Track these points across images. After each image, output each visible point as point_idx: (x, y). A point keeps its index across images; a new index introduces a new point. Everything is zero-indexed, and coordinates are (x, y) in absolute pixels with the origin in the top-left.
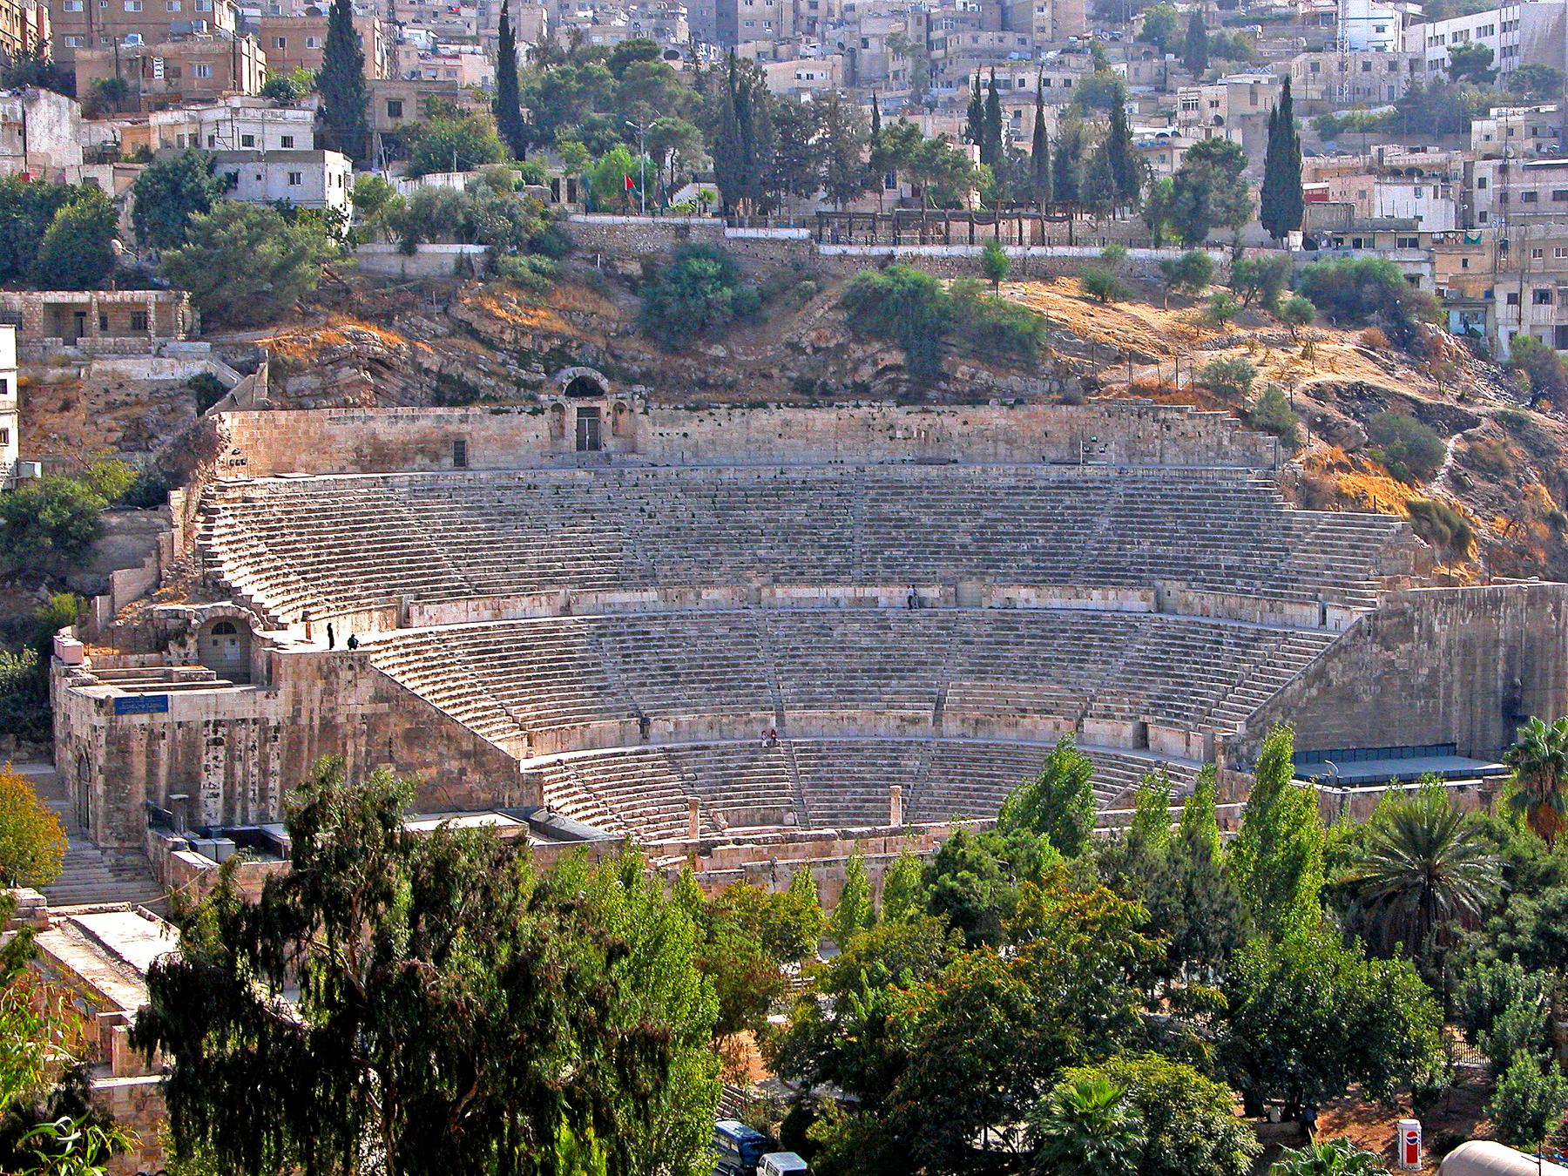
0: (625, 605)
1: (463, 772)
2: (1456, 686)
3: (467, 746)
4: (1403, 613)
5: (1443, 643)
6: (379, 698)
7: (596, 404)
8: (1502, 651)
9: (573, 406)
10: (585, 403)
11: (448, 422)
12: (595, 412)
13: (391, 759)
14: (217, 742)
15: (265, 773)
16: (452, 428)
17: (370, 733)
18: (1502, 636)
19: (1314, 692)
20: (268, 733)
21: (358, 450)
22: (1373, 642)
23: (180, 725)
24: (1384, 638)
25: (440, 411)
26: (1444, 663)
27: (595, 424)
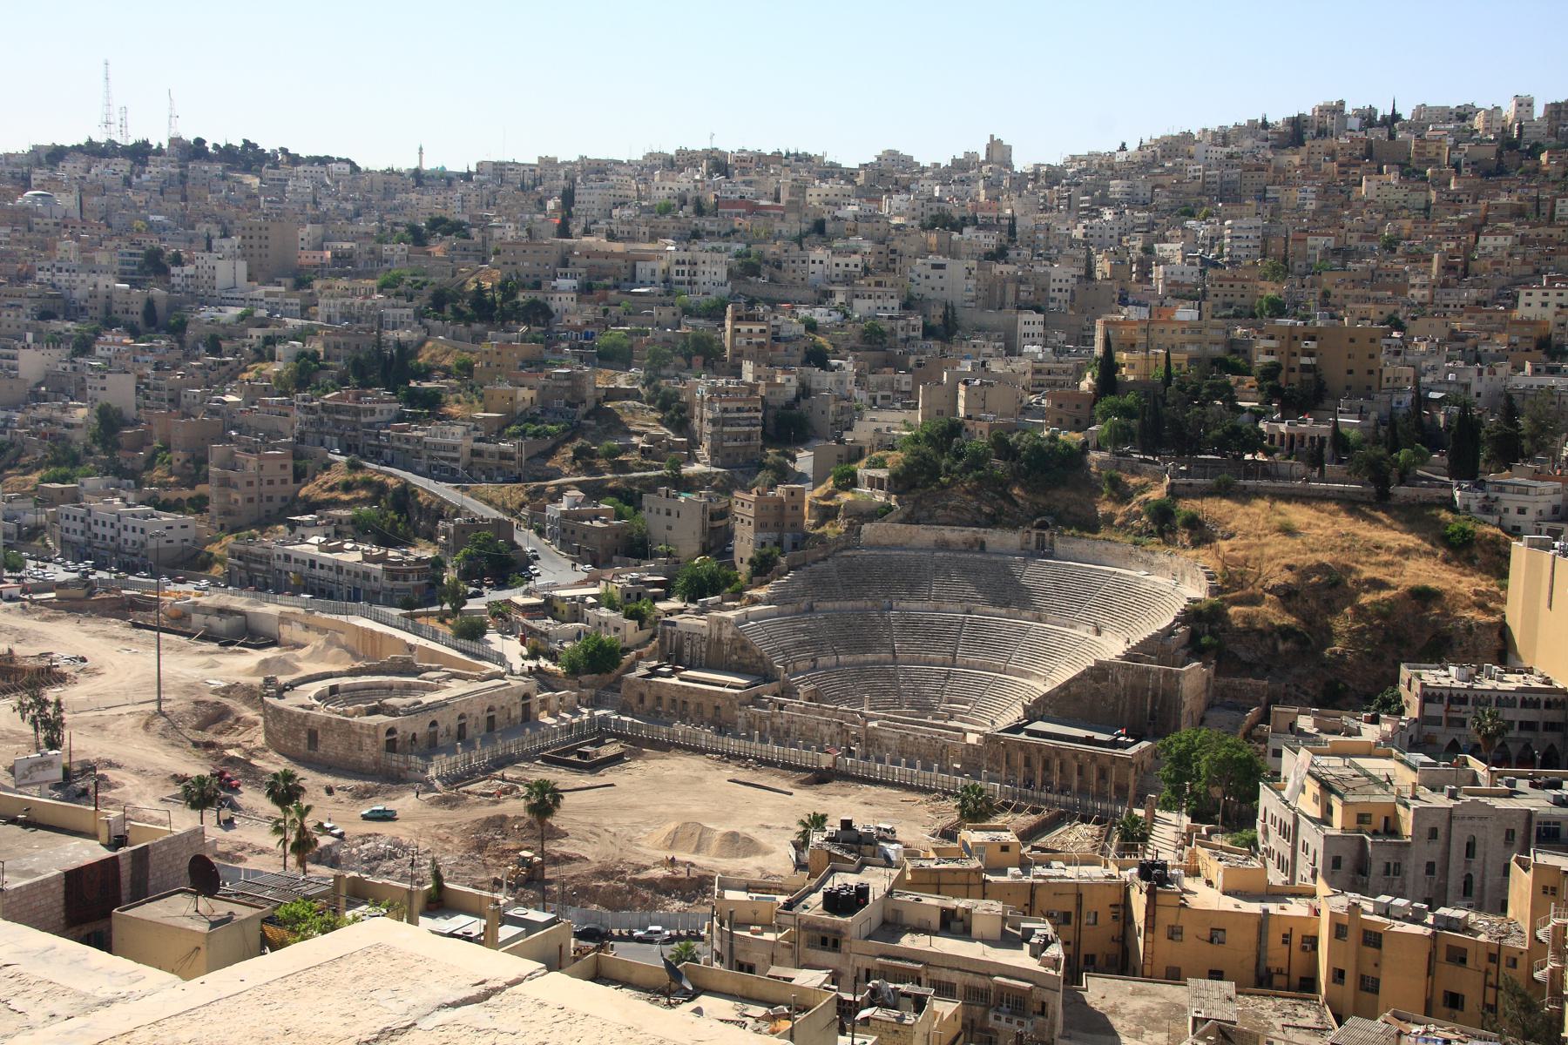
9: (1034, 532)
20: (703, 639)
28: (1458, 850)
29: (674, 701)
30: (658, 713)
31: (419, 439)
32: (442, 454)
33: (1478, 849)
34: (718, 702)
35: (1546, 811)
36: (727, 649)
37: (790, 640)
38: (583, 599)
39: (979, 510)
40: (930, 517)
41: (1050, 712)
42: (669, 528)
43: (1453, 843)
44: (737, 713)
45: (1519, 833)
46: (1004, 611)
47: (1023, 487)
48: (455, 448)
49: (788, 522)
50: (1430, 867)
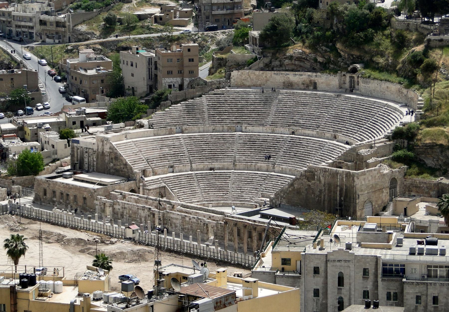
0: (309, 134)
1: (124, 168)
2: (326, 196)
3: (124, 162)
4: (313, 172)
5: (323, 183)
6: (110, 148)
7: (353, 75)
8: (338, 188)
9: (348, 75)
10: (350, 75)
11: (311, 77)
12: (353, 77)
13: (112, 162)
14: (86, 152)
15: (94, 161)
16: (312, 79)
17: (110, 155)
18: (339, 184)
19: (291, 189)
21: (284, 83)
22: (305, 179)
23: (81, 147)
24: (308, 178)
25: (309, 73)
26: (323, 188)
27: (354, 81)
28: (333, 281)
29: (62, 194)
30: (54, 202)
31: (9, 13)
32: (23, 24)
33: (346, 281)
34: (85, 194)
35: (405, 258)
36: (107, 158)
37: (156, 153)
38: (40, 126)
39: (316, 60)
40: (281, 66)
41: (284, 202)
42: (133, 75)
43: (329, 277)
44: (96, 202)
45: (371, 271)
46: (314, 133)
47: (344, 43)
48: (31, 19)
49: (186, 70)
50: (316, 293)
